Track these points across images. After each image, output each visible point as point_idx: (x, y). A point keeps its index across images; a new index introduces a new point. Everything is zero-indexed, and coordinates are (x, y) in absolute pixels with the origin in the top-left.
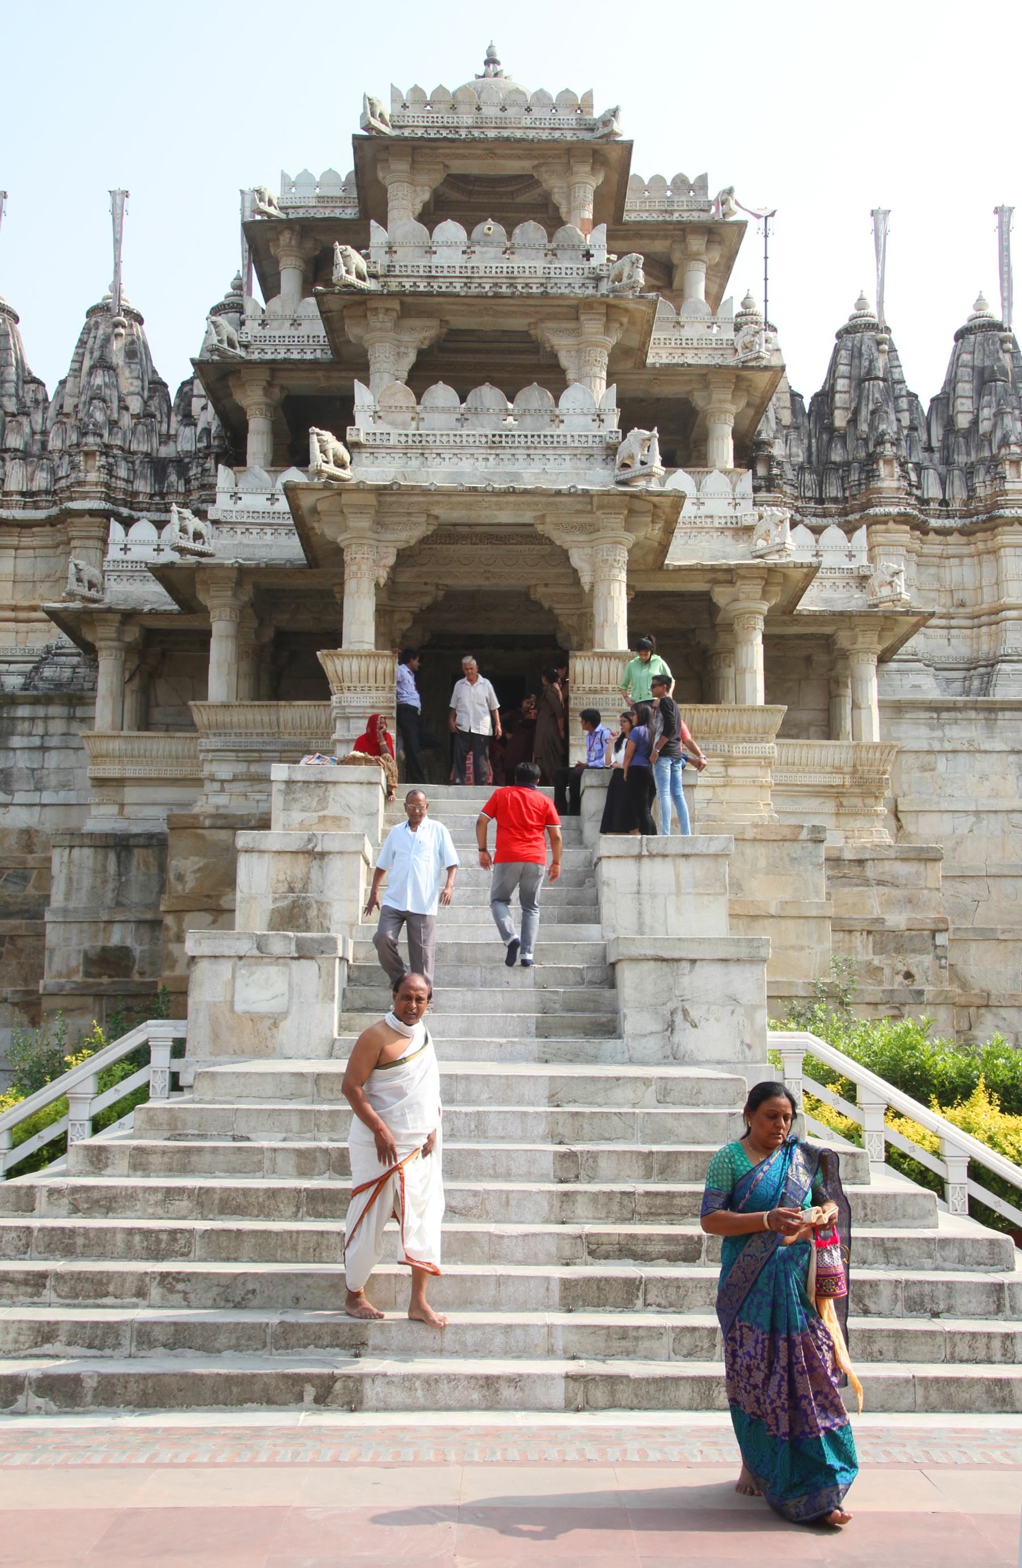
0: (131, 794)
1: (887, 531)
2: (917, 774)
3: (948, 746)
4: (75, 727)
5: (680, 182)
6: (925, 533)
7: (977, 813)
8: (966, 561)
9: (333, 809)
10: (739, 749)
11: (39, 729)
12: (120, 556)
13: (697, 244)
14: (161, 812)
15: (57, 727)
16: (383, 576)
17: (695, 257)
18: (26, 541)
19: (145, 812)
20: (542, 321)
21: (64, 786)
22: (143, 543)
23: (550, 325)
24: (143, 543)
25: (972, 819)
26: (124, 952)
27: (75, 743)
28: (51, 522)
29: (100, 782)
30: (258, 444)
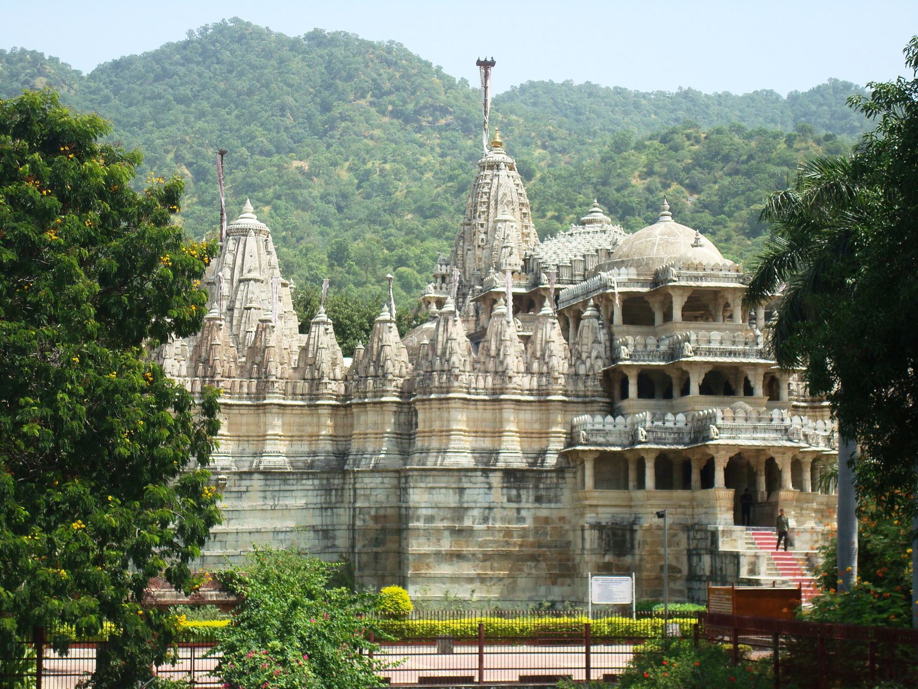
0: (600, 510)
4: (560, 481)
9: (734, 537)
10: (805, 505)
11: (548, 481)
12: (592, 428)
14: (609, 516)
15: (555, 480)
18: (529, 408)
19: (605, 516)
21: (556, 502)
22: (600, 423)
24: (600, 423)
26: (609, 563)
27: (561, 486)
28: (539, 401)
29: (591, 506)
30: (633, 390)
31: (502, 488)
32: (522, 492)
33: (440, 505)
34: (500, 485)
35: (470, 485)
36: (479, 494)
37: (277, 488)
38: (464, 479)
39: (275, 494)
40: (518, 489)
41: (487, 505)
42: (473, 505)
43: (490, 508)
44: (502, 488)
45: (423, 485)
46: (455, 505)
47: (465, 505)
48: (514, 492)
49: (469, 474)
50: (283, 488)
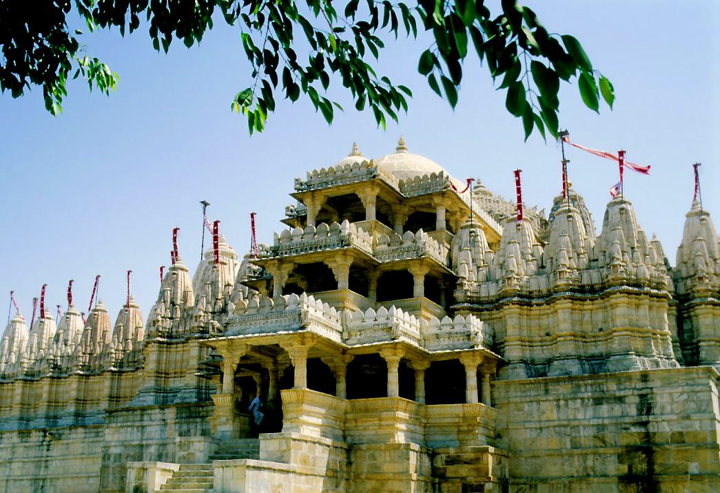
1: (510, 308)
2: (516, 412)
3: (528, 399)
5: (434, 176)
6: (532, 306)
7: (541, 429)
8: (550, 315)
13: (437, 200)
16: (235, 366)
17: (439, 205)
20: (326, 258)
23: (328, 260)
25: (539, 431)
31: (175, 423)
32: (192, 426)
33: (125, 443)
34: (174, 421)
35: (151, 423)
36: (157, 431)
37: (91, 440)
38: (146, 417)
39: (91, 444)
40: (188, 423)
41: (161, 442)
42: (150, 442)
43: (164, 445)
44: (175, 423)
45: (114, 425)
46: (135, 443)
47: (144, 443)
48: (185, 427)
49: (149, 412)
50: (95, 439)
